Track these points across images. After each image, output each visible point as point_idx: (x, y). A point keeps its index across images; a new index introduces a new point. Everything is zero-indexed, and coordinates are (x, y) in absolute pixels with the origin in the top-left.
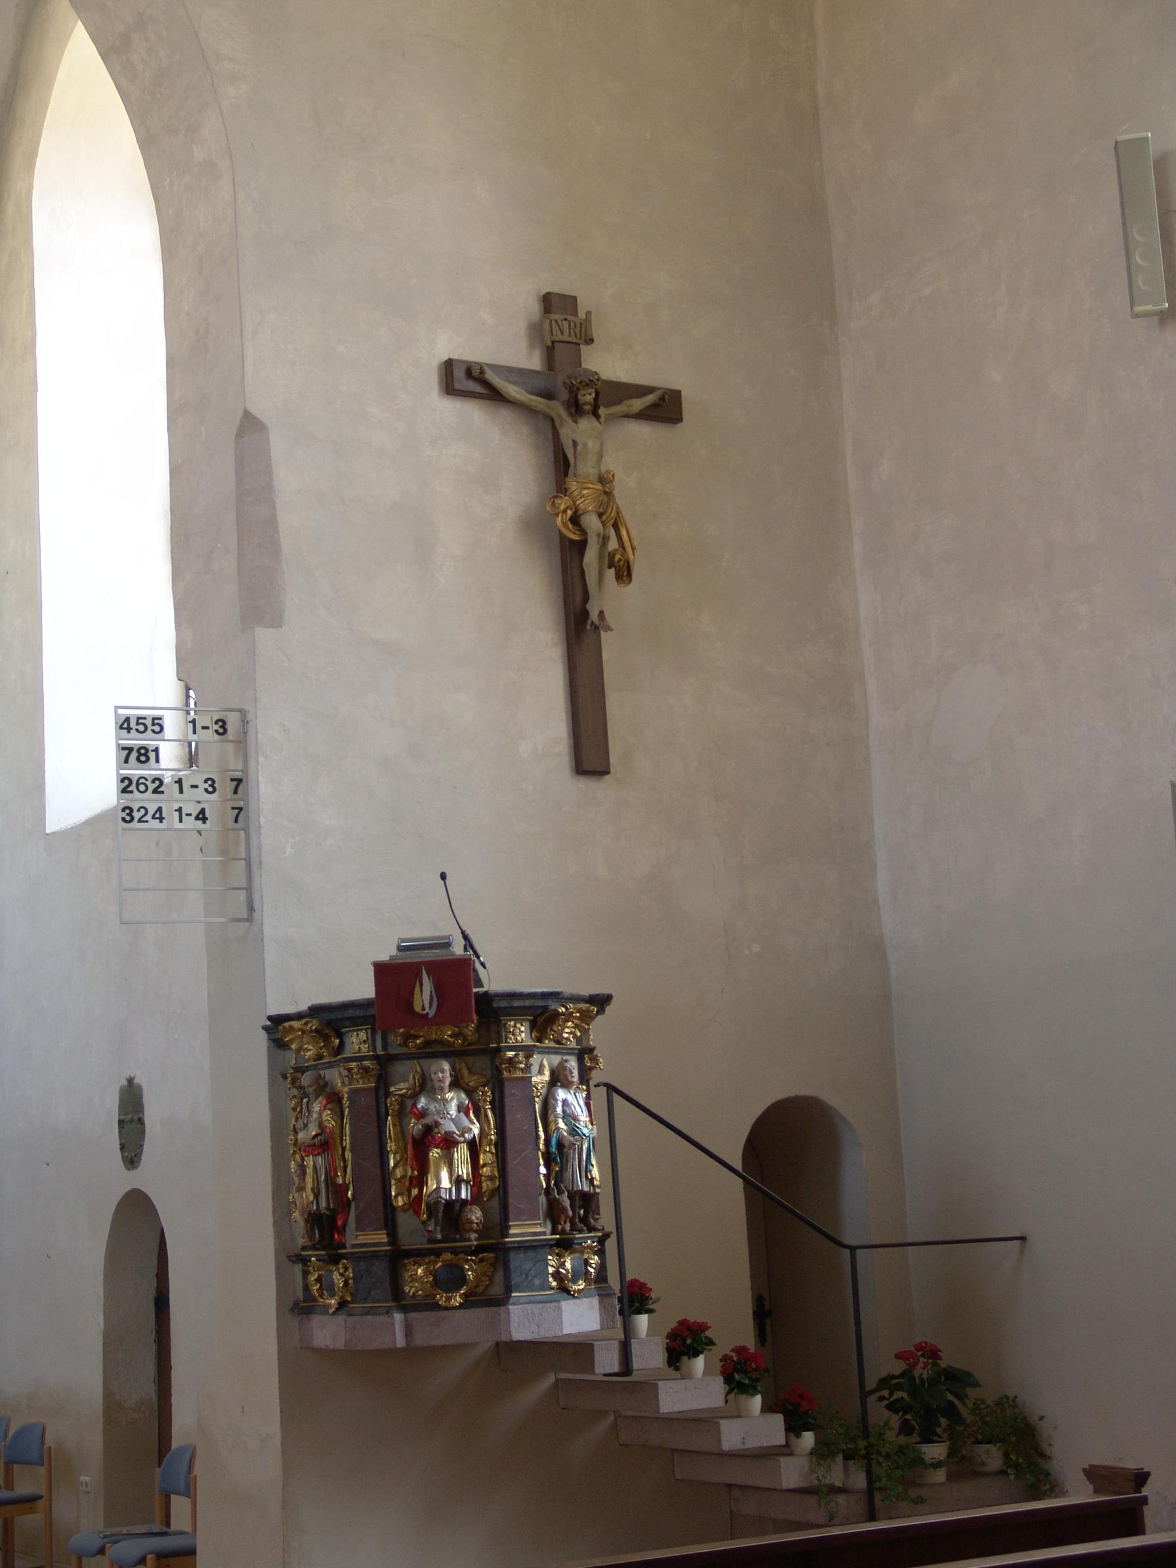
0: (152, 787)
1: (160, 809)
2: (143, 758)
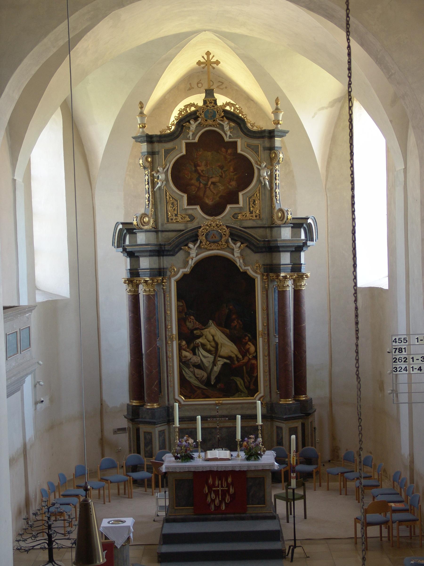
0: (403, 360)
1: (406, 367)
2: (400, 351)
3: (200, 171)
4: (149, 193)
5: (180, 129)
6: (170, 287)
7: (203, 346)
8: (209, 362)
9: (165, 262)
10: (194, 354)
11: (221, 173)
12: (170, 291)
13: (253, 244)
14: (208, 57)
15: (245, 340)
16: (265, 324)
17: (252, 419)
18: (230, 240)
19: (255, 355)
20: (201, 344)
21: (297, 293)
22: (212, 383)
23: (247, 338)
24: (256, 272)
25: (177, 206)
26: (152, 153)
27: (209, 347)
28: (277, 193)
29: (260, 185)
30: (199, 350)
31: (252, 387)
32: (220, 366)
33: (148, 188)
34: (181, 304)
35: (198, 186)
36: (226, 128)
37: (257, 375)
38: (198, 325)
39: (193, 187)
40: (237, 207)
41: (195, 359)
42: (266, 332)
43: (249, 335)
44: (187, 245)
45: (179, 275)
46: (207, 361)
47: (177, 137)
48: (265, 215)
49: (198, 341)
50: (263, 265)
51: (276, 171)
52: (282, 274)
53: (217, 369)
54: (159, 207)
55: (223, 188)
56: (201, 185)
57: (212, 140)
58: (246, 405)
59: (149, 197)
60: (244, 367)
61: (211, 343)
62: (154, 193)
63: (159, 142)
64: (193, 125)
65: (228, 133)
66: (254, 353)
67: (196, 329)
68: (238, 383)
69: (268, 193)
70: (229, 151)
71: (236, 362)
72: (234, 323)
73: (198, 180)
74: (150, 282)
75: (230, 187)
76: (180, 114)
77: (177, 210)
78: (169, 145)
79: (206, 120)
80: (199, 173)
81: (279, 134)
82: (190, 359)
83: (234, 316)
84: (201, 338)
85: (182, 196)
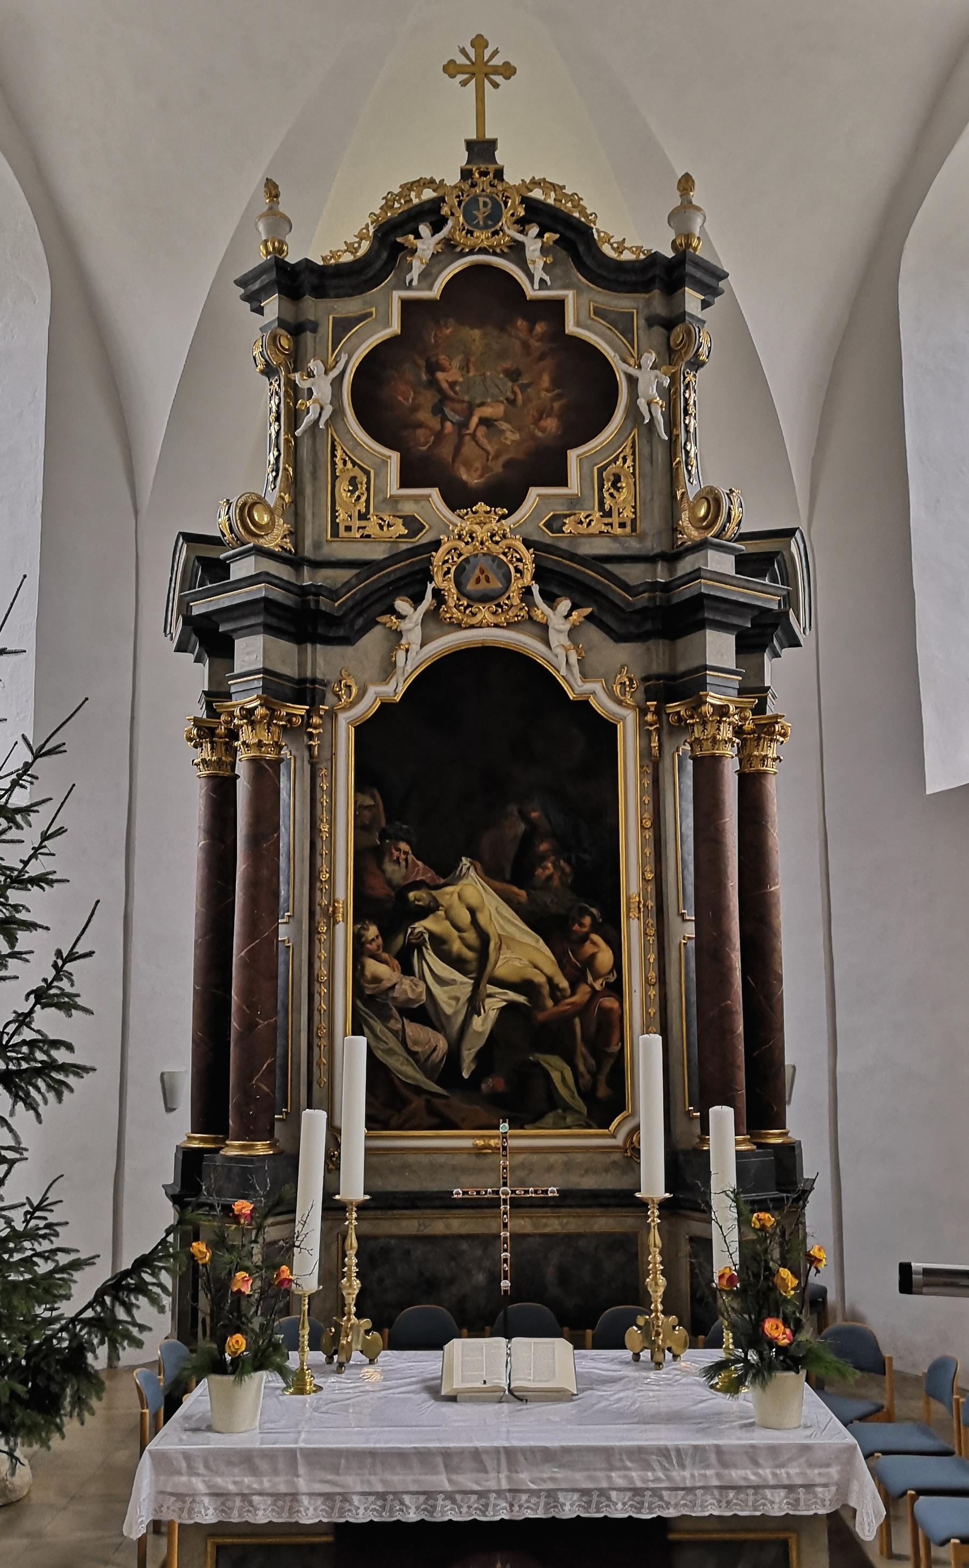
3: (445, 386)
4: (277, 446)
5: (385, 255)
6: (333, 745)
7: (439, 943)
8: (457, 999)
9: (320, 661)
10: (407, 970)
11: (514, 393)
12: (333, 755)
13: (614, 608)
14: (479, 55)
15: (581, 925)
16: (650, 876)
17: (602, 1206)
18: (536, 589)
19: (612, 979)
20: (431, 934)
21: (752, 785)
22: (466, 1075)
23: (587, 920)
24: (620, 703)
25: (368, 489)
26: (296, 329)
27: (457, 946)
28: (692, 454)
29: (636, 431)
30: (422, 957)
31: (603, 1091)
32: (493, 1014)
33: (278, 433)
34: (369, 802)
35: (438, 427)
36: (533, 247)
37: (622, 1050)
38: (422, 871)
39: (420, 432)
40: (560, 495)
41: (408, 989)
42: (651, 903)
43: (594, 911)
44: (392, 611)
45: (367, 707)
46: (450, 998)
47: (376, 281)
48: (651, 524)
49: (419, 926)
50: (645, 679)
51: (687, 387)
52: (713, 698)
53: (482, 1024)
54: (308, 490)
55: (517, 436)
56: (448, 425)
57: (485, 294)
58: (580, 1157)
59: (277, 459)
60: (577, 1021)
61: (465, 935)
62: (294, 455)
63: (320, 292)
64: (426, 243)
65: (539, 274)
66: (611, 971)
67: (416, 885)
68: (555, 1076)
69: (660, 454)
70: (540, 328)
71: (550, 1003)
72: (546, 868)
73: (438, 410)
74: (261, 711)
75: (540, 434)
76: (388, 206)
77: (368, 501)
78: (350, 307)
79: (470, 232)
80: (440, 390)
81: (699, 274)
82: (393, 987)
83: (544, 847)
84: (431, 917)
85: (385, 462)
